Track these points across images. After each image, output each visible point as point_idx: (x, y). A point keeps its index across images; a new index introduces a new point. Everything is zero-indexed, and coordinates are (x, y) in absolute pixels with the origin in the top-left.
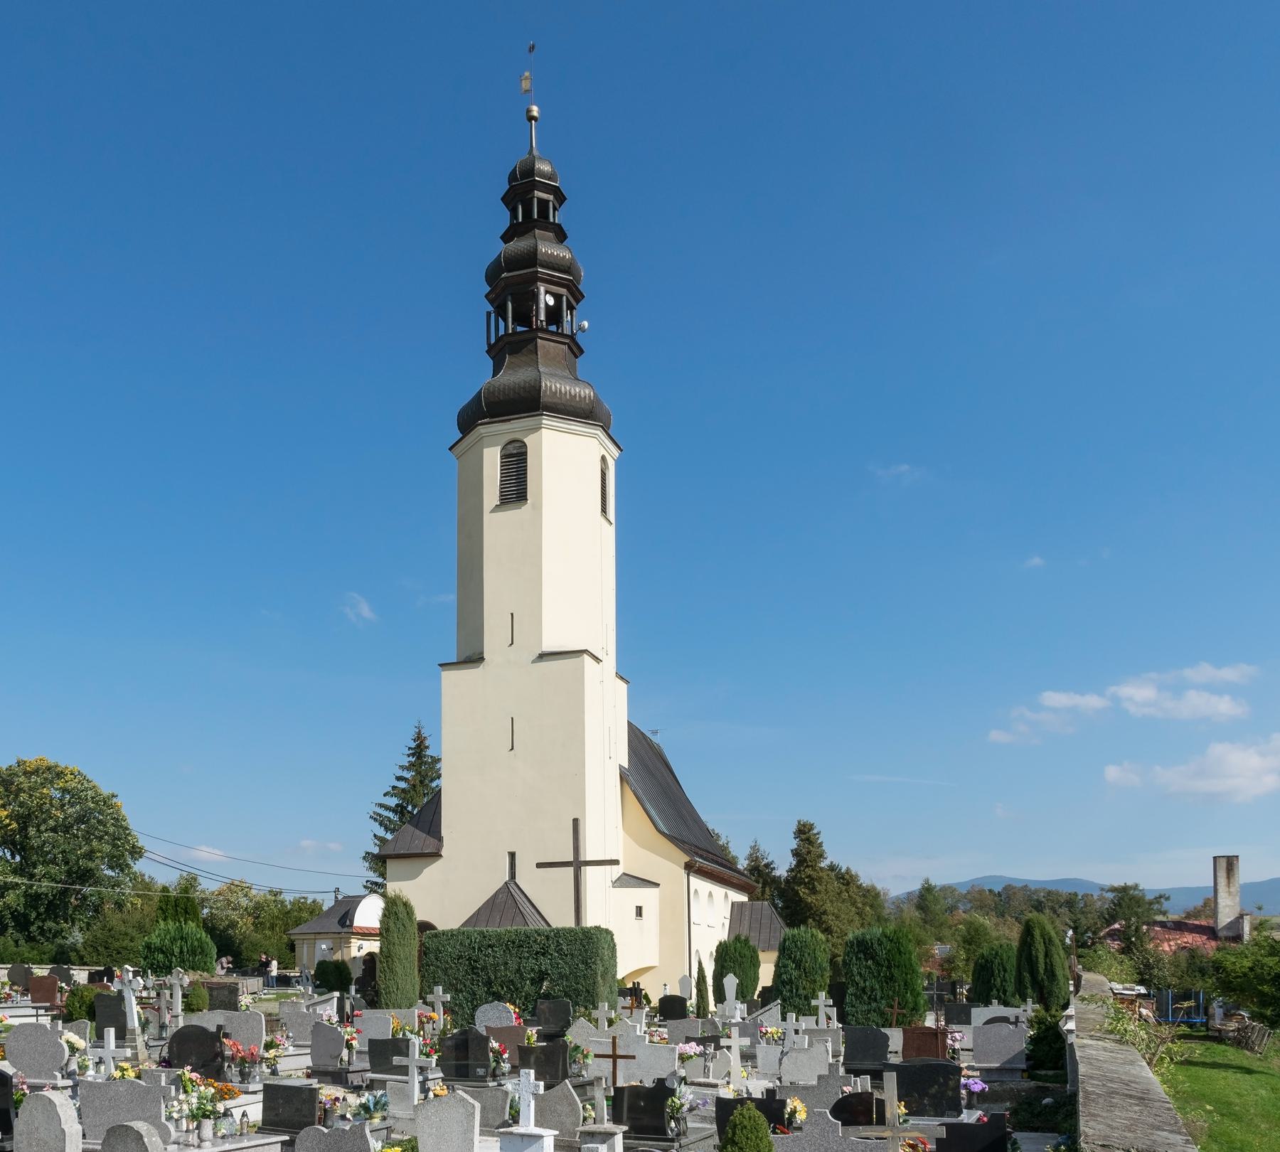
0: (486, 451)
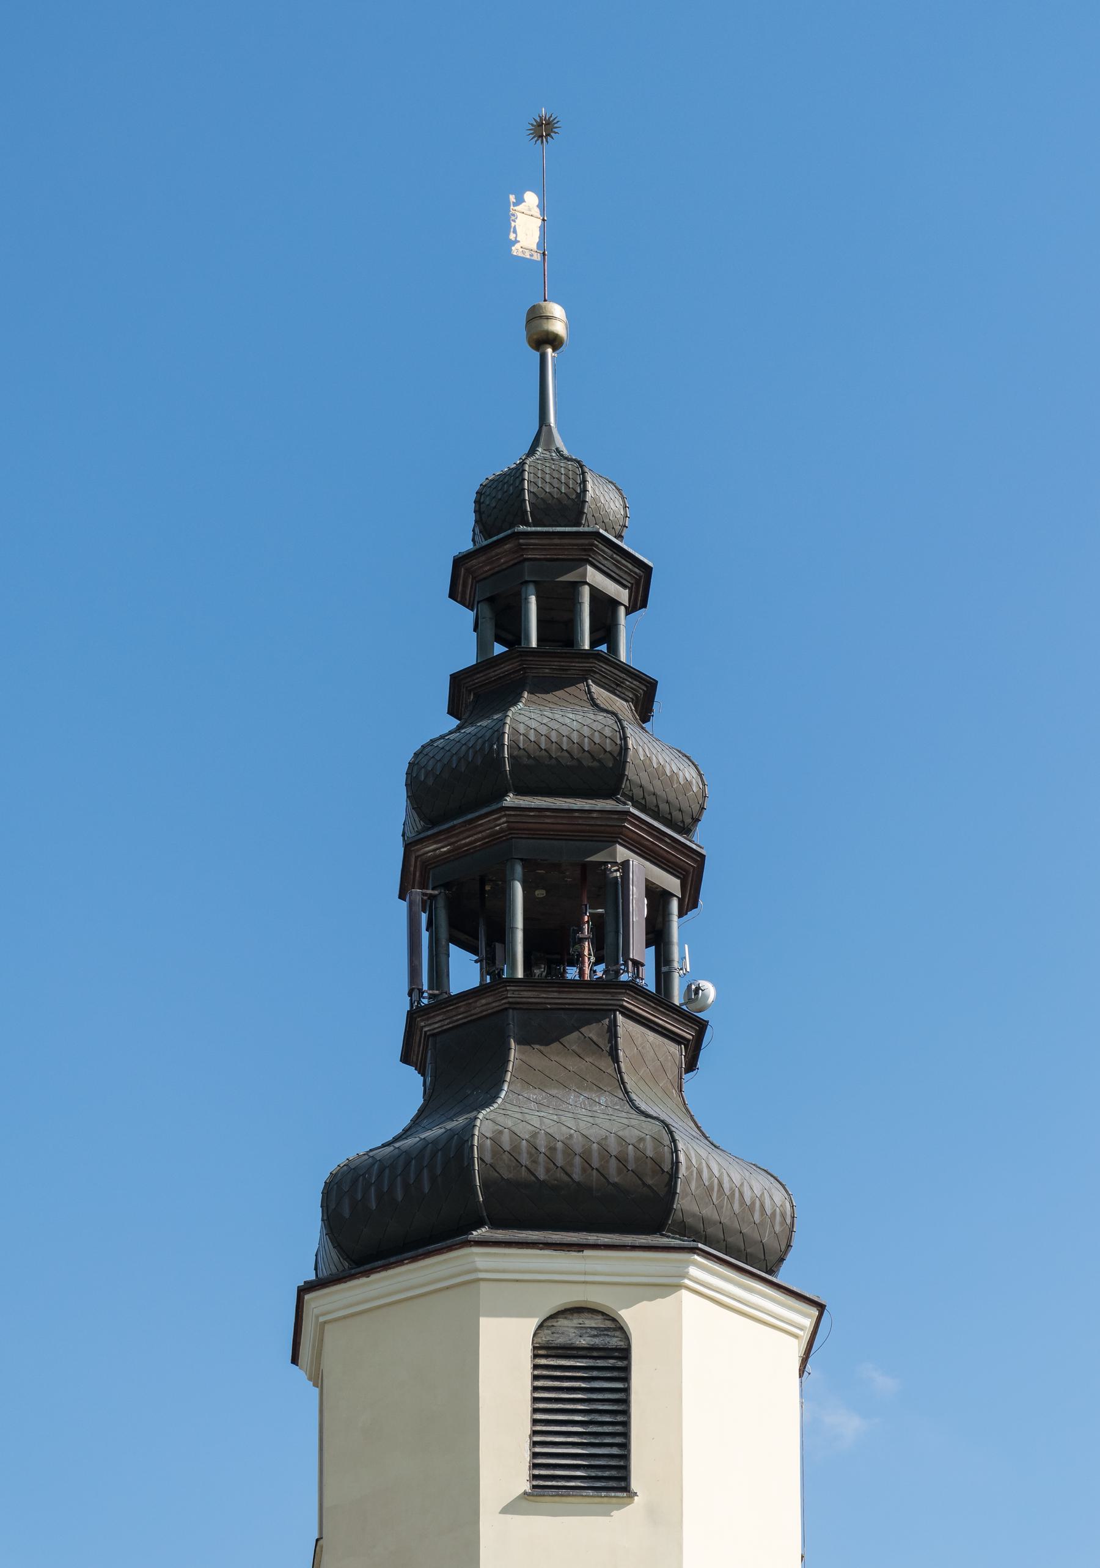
0: (484, 1321)
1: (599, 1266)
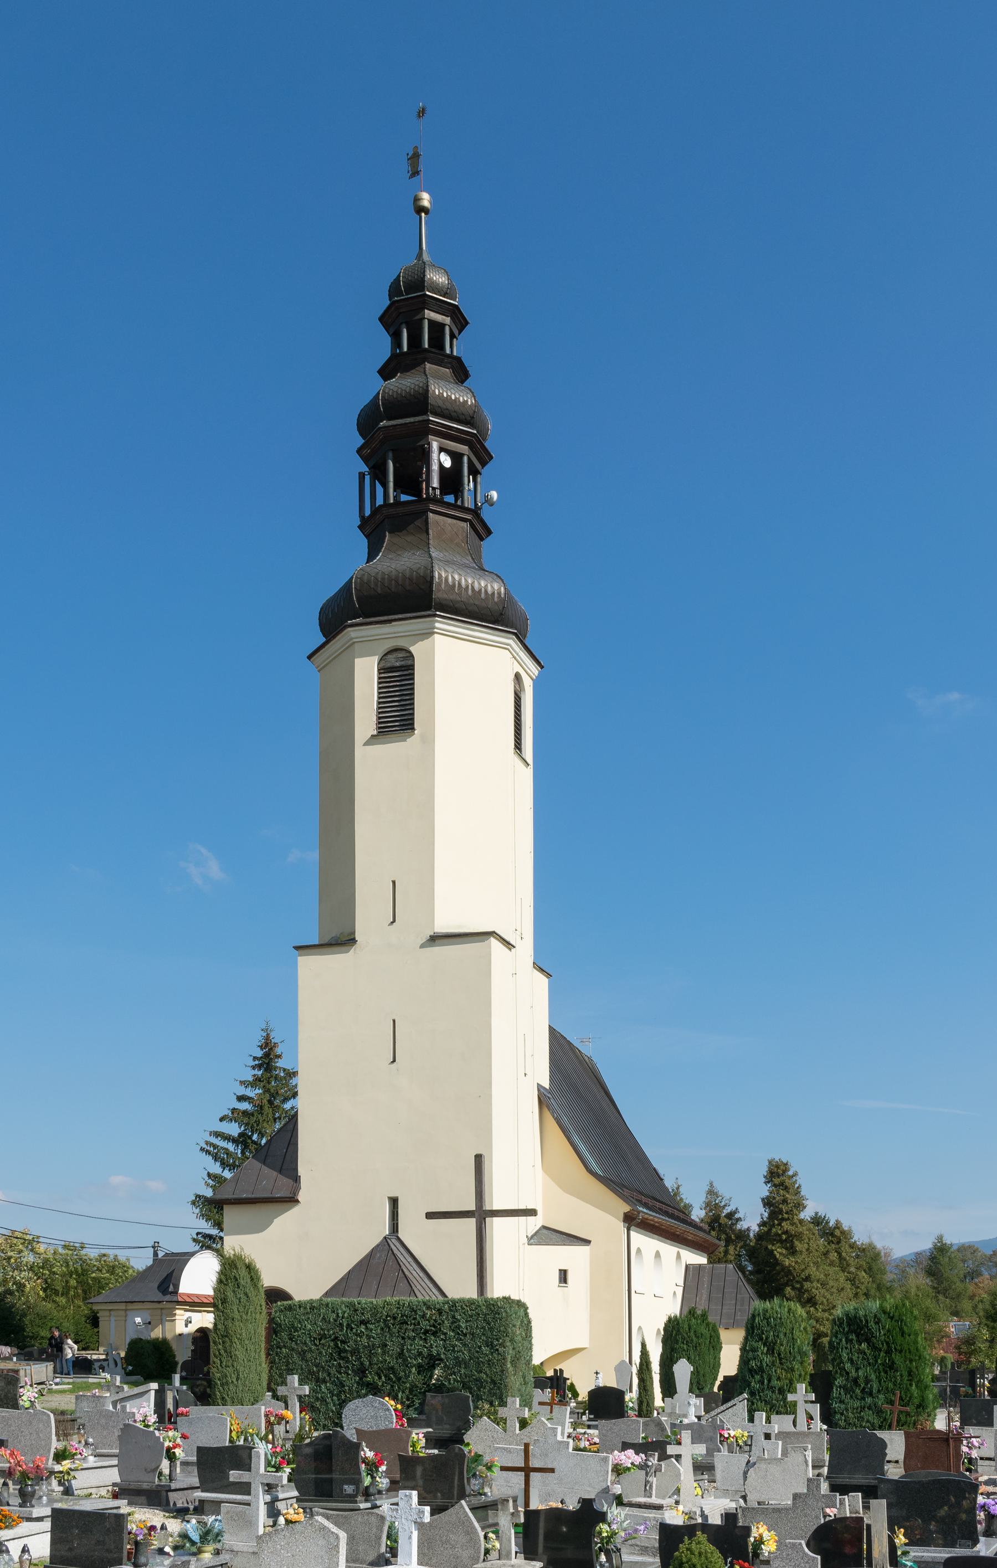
0: (357, 661)
1: (400, 629)
